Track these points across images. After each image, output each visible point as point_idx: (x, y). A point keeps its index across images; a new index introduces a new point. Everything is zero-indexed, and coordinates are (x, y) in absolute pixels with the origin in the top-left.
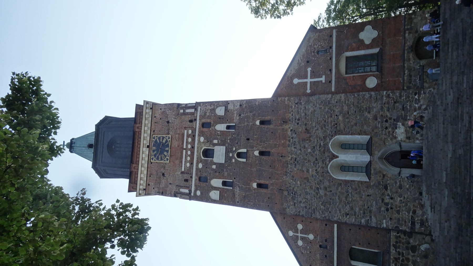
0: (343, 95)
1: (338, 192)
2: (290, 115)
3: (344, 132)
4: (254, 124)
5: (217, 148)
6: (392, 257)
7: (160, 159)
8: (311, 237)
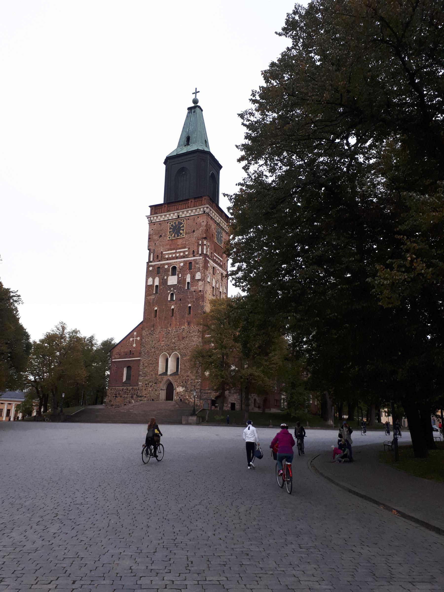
5: (176, 277)
7: (170, 230)
8: (134, 345)
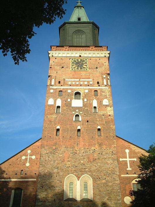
0: (119, 182)
2: (105, 148)
4: (98, 125)
7: (72, 64)
8: (28, 164)
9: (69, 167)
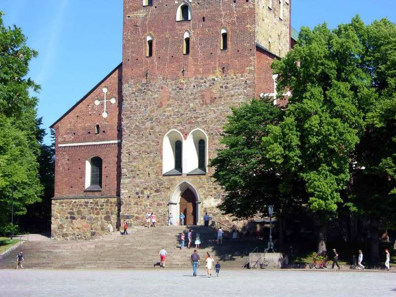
1: (150, 142)
3: (211, 144)
6: (98, 199)
8: (105, 115)
9: (171, 116)
